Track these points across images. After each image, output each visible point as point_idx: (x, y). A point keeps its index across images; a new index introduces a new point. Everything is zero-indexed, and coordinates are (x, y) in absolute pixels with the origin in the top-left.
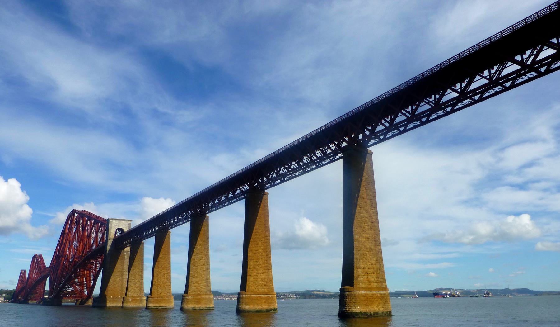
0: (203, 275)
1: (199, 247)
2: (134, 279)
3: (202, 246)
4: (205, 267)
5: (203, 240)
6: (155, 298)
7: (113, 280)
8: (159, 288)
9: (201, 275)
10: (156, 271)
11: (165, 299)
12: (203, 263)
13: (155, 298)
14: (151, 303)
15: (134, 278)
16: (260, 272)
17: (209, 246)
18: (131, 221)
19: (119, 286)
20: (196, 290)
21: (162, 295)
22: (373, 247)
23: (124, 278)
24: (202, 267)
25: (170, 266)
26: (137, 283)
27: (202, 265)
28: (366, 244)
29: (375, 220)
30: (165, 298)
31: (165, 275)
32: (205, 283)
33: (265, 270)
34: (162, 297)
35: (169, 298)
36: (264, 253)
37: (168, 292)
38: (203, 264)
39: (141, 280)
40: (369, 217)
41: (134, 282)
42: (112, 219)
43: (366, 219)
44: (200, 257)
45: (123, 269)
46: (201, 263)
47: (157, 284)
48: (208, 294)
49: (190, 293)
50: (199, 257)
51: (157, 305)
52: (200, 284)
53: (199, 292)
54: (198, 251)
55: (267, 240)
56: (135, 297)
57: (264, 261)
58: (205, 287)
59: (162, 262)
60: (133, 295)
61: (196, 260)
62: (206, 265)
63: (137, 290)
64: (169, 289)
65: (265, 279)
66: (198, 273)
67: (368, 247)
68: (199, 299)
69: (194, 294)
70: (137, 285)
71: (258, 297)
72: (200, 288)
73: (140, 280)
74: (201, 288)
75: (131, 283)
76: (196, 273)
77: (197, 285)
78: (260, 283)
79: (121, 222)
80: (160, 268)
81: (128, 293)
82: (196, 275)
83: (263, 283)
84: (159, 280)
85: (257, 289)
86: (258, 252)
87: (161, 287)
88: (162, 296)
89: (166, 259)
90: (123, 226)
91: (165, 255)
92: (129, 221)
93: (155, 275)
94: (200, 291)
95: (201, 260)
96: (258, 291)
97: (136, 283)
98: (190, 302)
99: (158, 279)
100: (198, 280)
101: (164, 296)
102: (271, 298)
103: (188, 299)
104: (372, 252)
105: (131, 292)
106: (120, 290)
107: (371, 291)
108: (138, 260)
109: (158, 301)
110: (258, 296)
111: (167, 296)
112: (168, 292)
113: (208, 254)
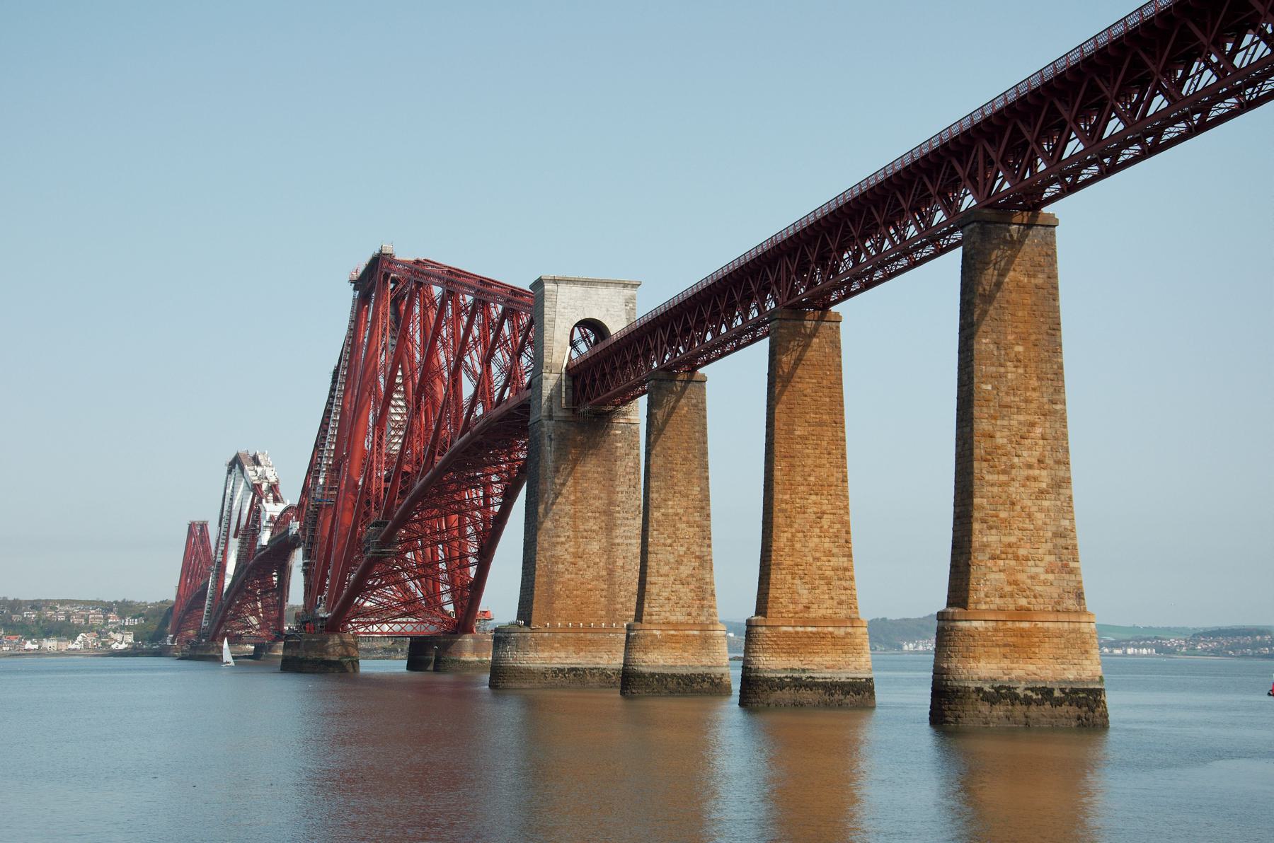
0: (1040, 517)
1: (1010, 376)
2: (669, 541)
3: (1026, 367)
4: (1044, 473)
5: (1033, 337)
6: (785, 629)
7: (572, 550)
8: (797, 581)
9: (1030, 516)
10: (782, 501)
11: (831, 633)
12: (1036, 454)
13: (785, 629)
14: (765, 650)
15: (669, 537)
17: (1061, 367)
18: (635, 286)
19: (597, 578)
20: (1008, 589)
21: (816, 612)
23: (617, 541)
24: (1031, 472)
25: (844, 480)
26: (685, 560)
27: (1030, 466)
30: (830, 629)
31: (826, 522)
34: (814, 622)
35: (850, 630)
37: (841, 603)
38: (1034, 460)
39: (701, 546)
41: (672, 558)
42: (555, 281)
44: (1020, 423)
45: (611, 503)
46: (1025, 454)
47: (788, 561)
48: (1068, 611)
49: (977, 603)
50: (1014, 423)
51: (795, 663)
53: (1023, 602)
54: (1007, 394)
56: (676, 626)
58: (1053, 572)
59: (810, 462)
60: (668, 614)
61: (1000, 440)
62: (1049, 462)
63: (686, 593)
64: (846, 589)
66: (1013, 504)
68: (1022, 633)
69: (1000, 610)
70: (685, 571)
72: (1029, 581)
73: (695, 548)
74: (1032, 578)
75: (658, 561)
76: (1003, 504)
77: (1013, 563)
79: (592, 291)
80: (801, 488)
81: (646, 605)
82: (1003, 515)
84: (798, 546)
87: (807, 579)
88: (814, 620)
89: (824, 443)
90: (604, 309)
91: (821, 424)
92: (625, 285)
93: (779, 519)
94: (1028, 593)
95: (1022, 437)
97: (679, 563)
98: (981, 650)
99: (791, 541)
100: (1013, 539)
101: (824, 617)
103: (970, 634)
105: (662, 601)
106: (604, 593)
108: (685, 459)
109: (797, 645)
111: (837, 623)
112: (841, 603)
113: (1058, 407)
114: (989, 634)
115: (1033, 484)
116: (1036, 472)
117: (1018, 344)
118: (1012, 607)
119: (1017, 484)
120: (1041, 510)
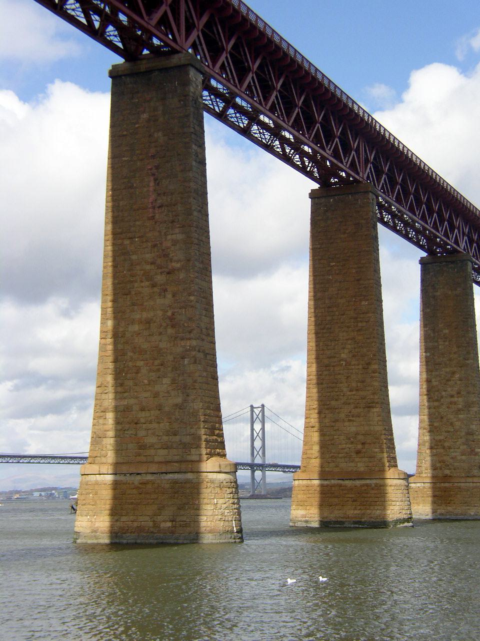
0: (458, 424)
1: (440, 347)
4: (460, 399)
9: (452, 424)
16: (342, 416)
22: (163, 345)
24: (453, 399)
27: (452, 396)
28: (139, 341)
29: (178, 265)
32: (464, 444)
33: (358, 410)
36: (353, 363)
40: (159, 261)
43: (148, 267)
44: (446, 373)
46: (449, 389)
52: (450, 448)
53: (447, 472)
55: (364, 324)
57: (354, 385)
65: (357, 434)
66: (442, 418)
67: (145, 346)
71: (334, 486)
72: (451, 460)
74: (452, 458)
78: (340, 447)
83: (350, 446)
85: (332, 465)
86: (336, 360)
94: (450, 466)
96: (337, 470)
100: (442, 438)
102: (373, 489)
104: (157, 362)
107: (138, 474)
110: (333, 482)
114: (425, 490)
115: (453, 406)
116: (455, 399)
117: (445, 329)
118: (441, 475)
119: (444, 407)
120: (459, 420)
